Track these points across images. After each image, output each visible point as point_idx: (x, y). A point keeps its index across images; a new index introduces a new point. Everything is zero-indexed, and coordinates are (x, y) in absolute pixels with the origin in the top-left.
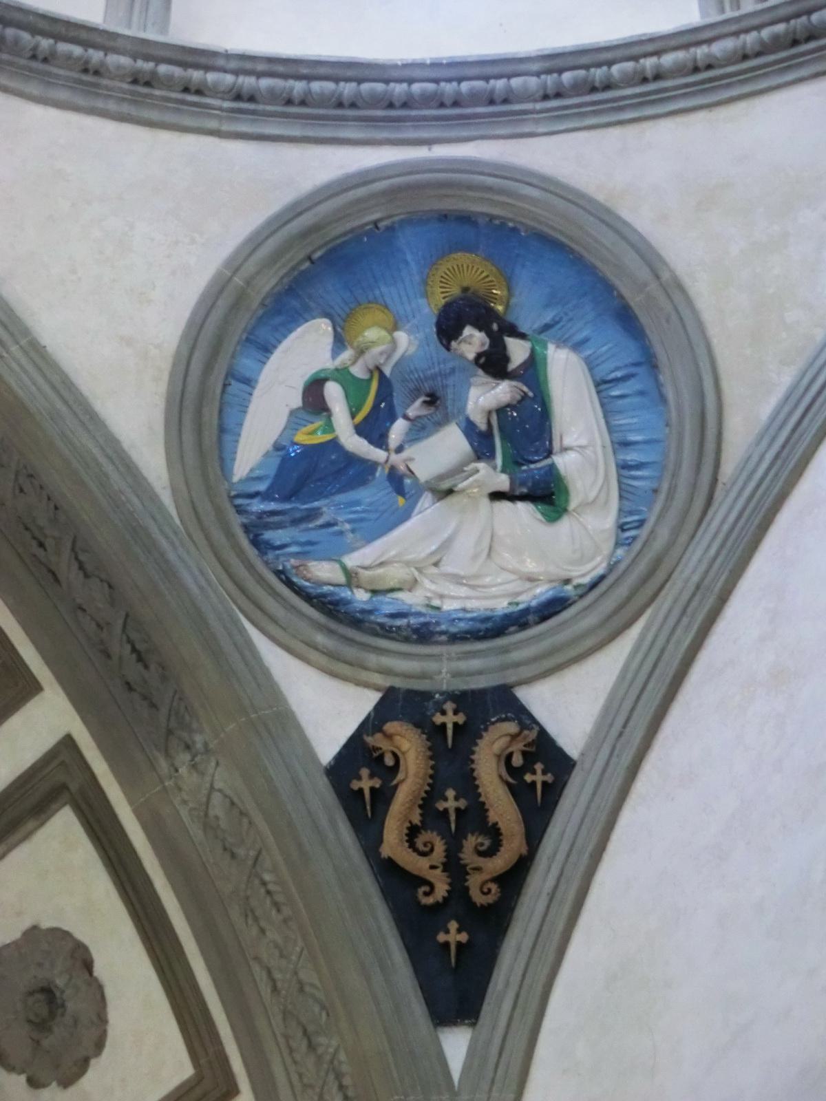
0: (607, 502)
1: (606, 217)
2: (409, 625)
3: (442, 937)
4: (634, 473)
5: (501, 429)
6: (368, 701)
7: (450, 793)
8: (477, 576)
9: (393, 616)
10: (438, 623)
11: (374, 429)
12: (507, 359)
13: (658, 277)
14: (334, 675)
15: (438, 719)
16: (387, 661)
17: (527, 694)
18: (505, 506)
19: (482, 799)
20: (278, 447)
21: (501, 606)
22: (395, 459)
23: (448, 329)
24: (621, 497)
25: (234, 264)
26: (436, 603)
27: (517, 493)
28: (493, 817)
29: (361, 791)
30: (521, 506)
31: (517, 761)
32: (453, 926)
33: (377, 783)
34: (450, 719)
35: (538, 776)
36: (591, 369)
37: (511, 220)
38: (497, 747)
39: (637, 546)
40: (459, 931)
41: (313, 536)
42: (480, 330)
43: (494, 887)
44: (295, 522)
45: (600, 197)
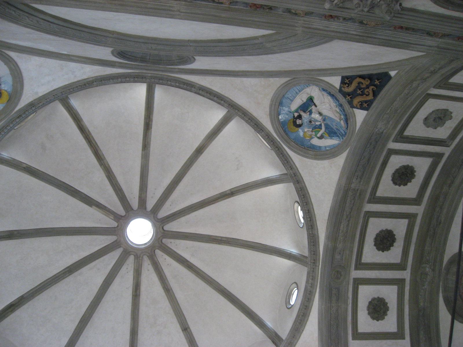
0: (305, 91)
1: (270, 114)
2: (341, 108)
3: (378, 84)
4: (299, 89)
5: (307, 110)
6: (354, 109)
7: (358, 92)
8: (328, 103)
9: (341, 111)
10: (338, 105)
11: (320, 127)
12: (298, 115)
13: (272, 103)
14: (355, 115)
15: (350, 99)
16: (348, 109)
17: (338, 88)
18: (316, 104)
19: (356, 87)
20: (331, 139)
21: (329, 97)
22: (321, 121)
23: (300, 126)
24: (304, 89)
25: (312, 158)
26: (336, 106)
27: (313, 104)
28: (357, 85)
29: (367, 105)
30: (315, 102)
31: (347, 85)
32: (376, 83)
33: (364, 104)
34: (349, 98)
35: (347, 81)
36: (291, 103)
37: (281, 126)
38: (347, 89)
39: (309, 84)
40: (376, 82)
41: (339, 127)
42: (296, 122)
43: (366, 80)
44: (339, 130)
45: (269, 116)
